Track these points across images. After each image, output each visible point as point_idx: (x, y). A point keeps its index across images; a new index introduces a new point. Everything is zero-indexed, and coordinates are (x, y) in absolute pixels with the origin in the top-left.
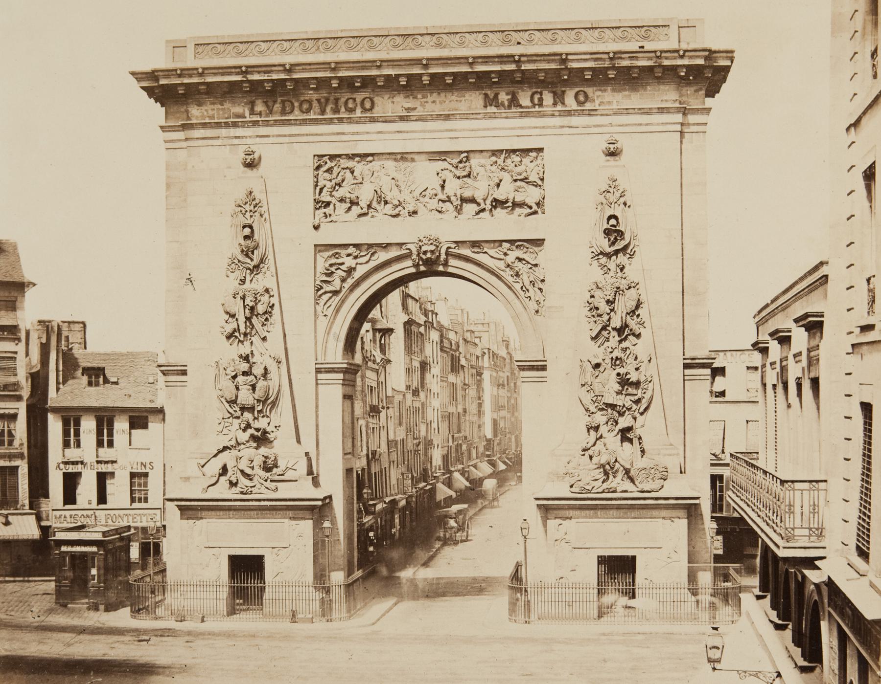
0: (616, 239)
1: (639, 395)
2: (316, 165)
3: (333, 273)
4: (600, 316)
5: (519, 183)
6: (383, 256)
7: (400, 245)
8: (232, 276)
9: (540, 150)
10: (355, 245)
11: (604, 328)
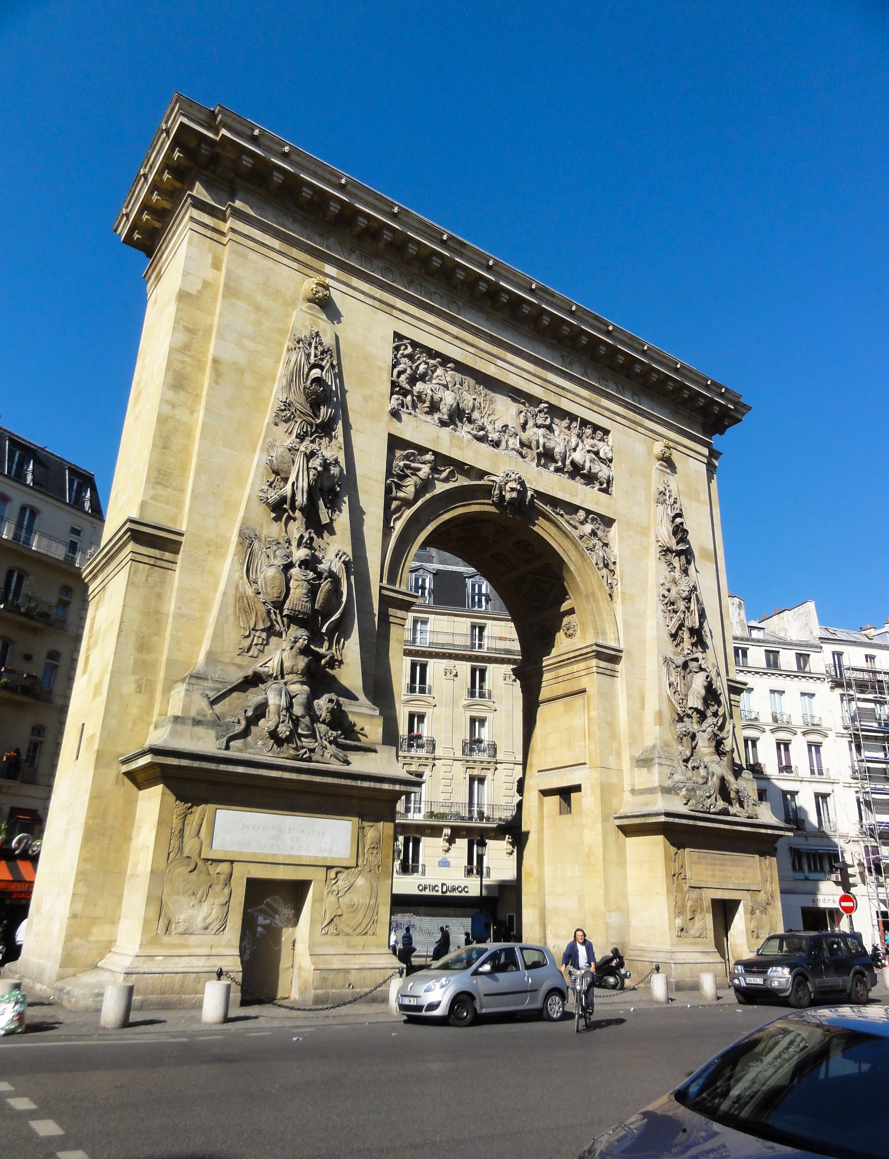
3: (407, 476)
6: (462, 481)
7: (482, 474)
9: (606, 432)
10: (435, 453)
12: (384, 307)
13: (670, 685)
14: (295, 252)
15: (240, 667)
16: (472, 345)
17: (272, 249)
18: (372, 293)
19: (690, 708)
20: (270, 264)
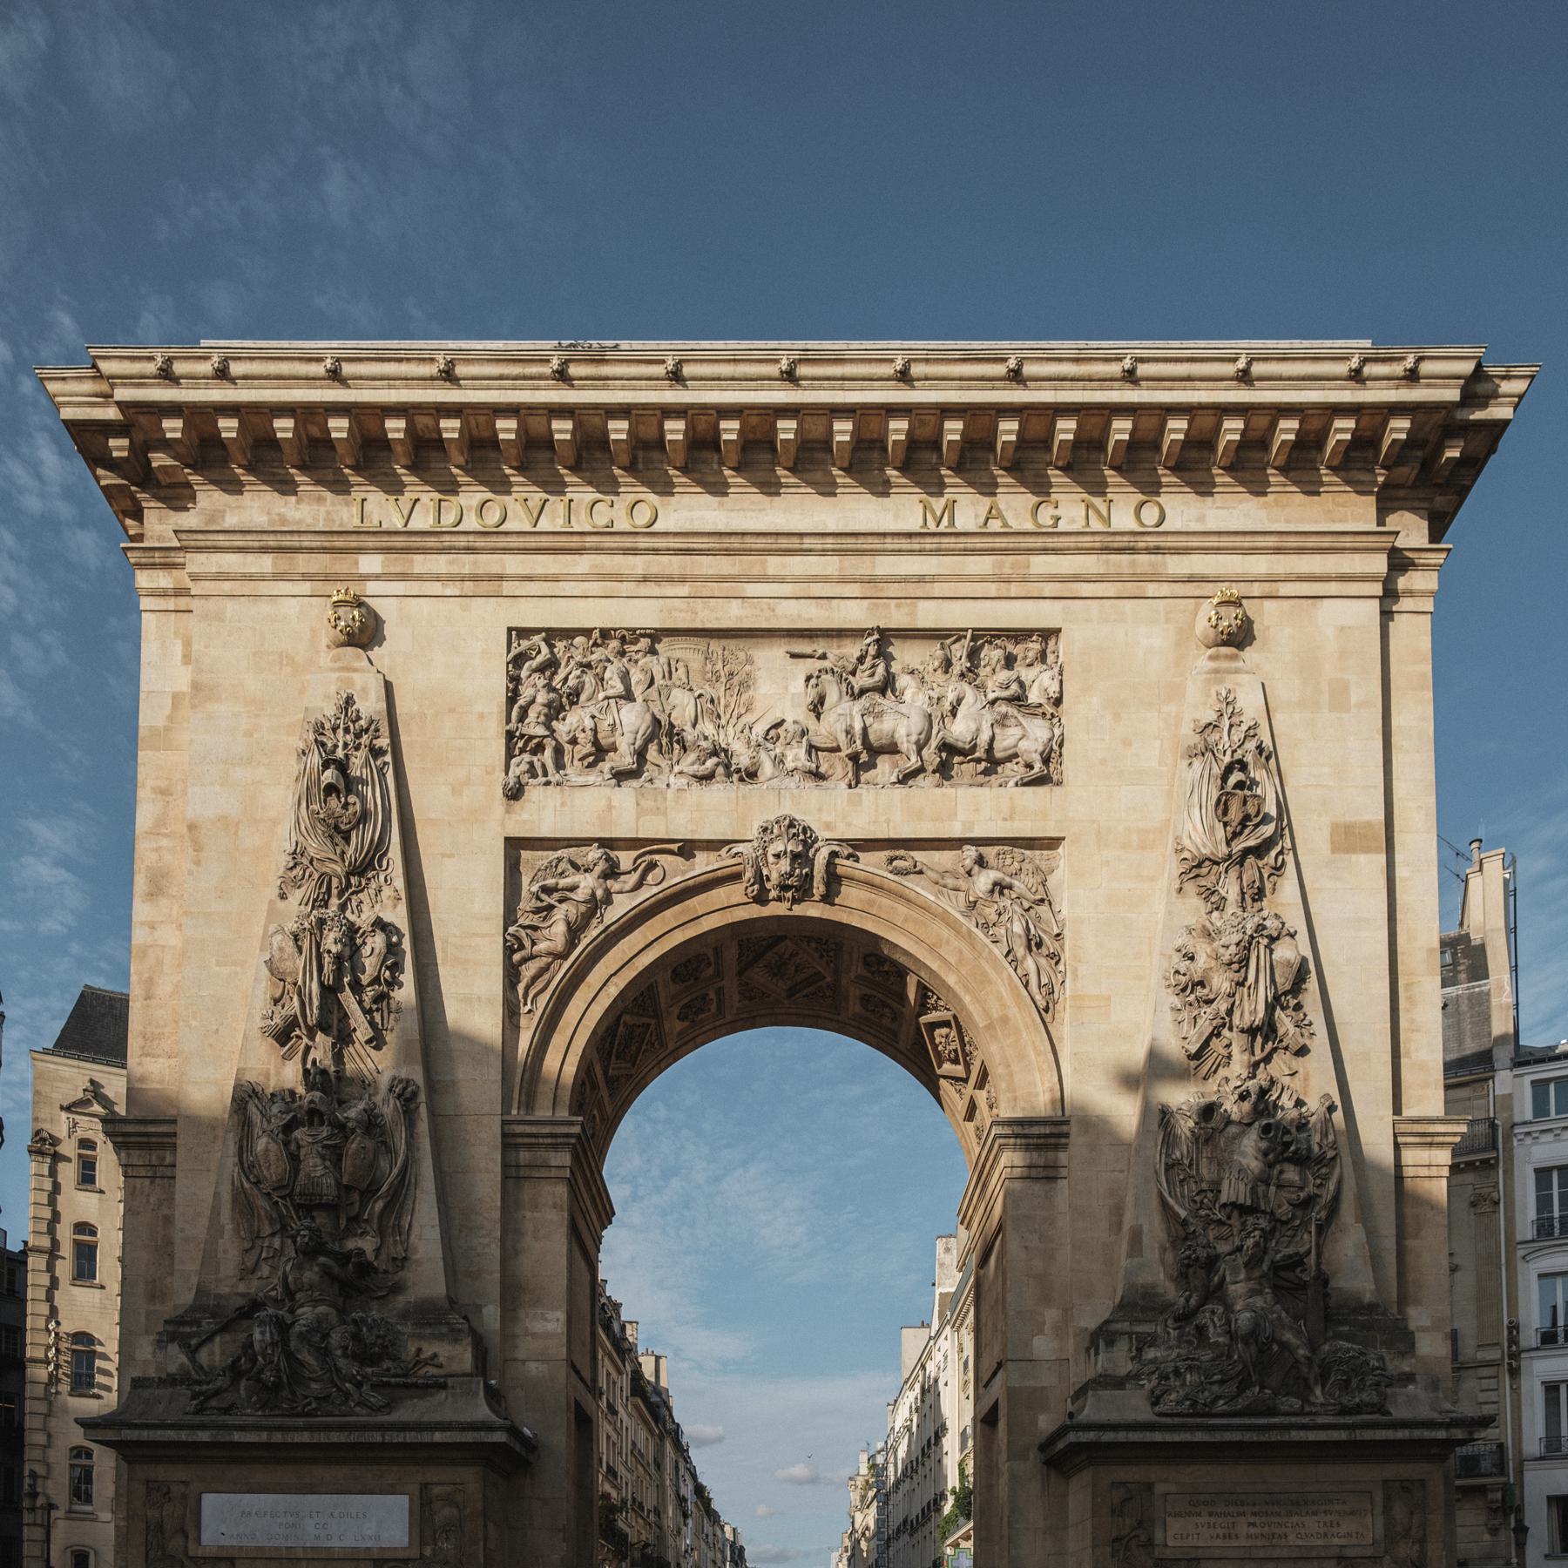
0: (1243, 824)
1: (1310, 1189)
2: (514, 652)
4: (1209, 1002)
5: (1003, 708)
8: (296, 896)
11: (1215, 1033)
12: (485, 587)
13: (1169, 1167)
14: (303, 563)
15: (243, 1295)
16: (683, 580)
17: (262, 578)
18: (455, 569)
19: (1224, 1206)
20: (265, 607)
